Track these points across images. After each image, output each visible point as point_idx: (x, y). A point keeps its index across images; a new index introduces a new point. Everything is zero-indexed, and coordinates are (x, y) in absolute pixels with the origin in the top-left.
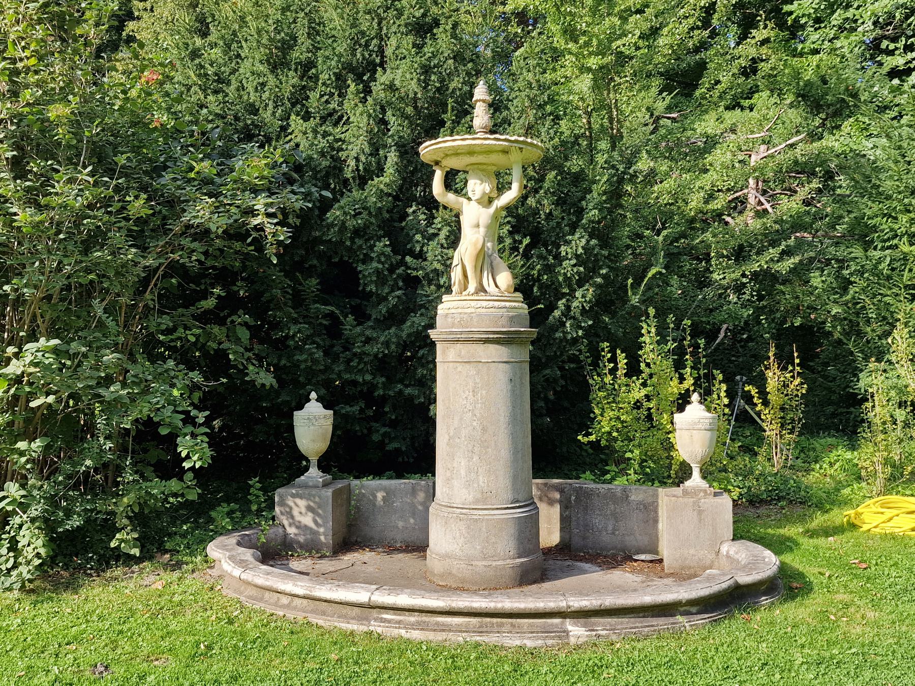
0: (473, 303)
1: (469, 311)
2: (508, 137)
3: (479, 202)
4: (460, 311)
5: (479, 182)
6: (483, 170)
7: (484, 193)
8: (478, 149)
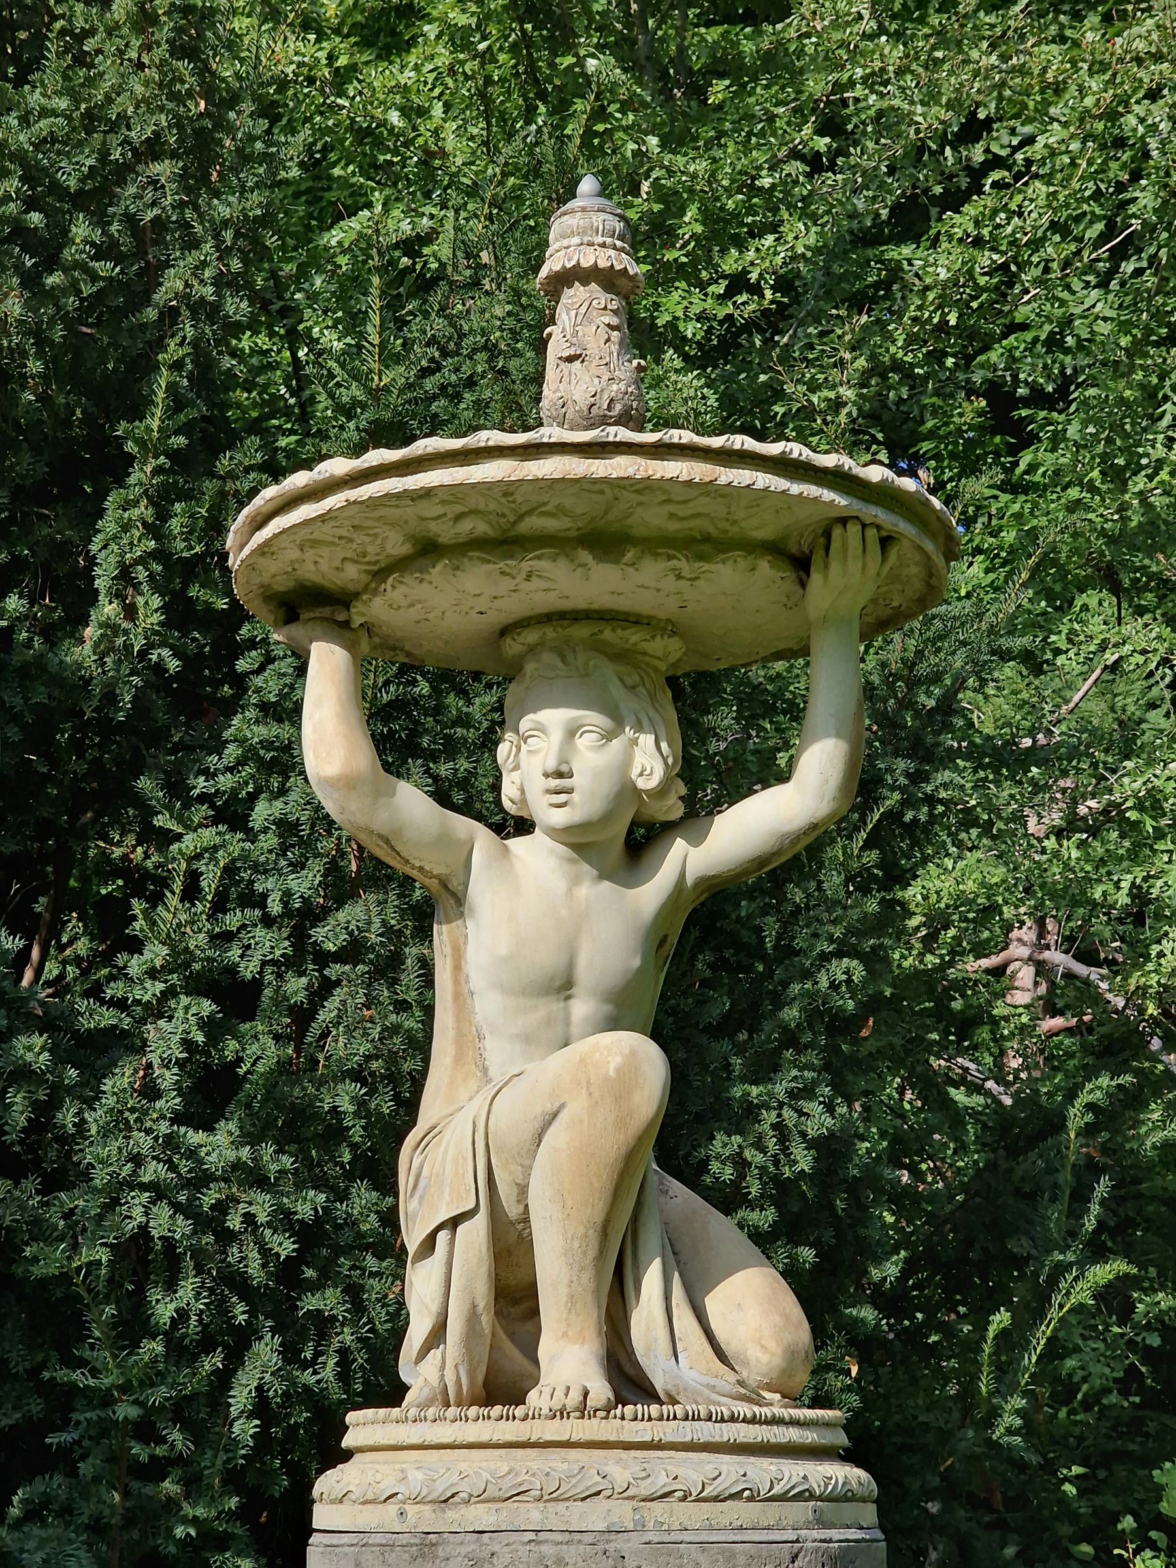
0: (620, 1469)
1: (595, 1516)
2: (797, 450)
3: (580, 842)
4: (532, 1515)
5: (595, 719)
6: (621, 656)
7: (627, 791)
8: (651, 518)
